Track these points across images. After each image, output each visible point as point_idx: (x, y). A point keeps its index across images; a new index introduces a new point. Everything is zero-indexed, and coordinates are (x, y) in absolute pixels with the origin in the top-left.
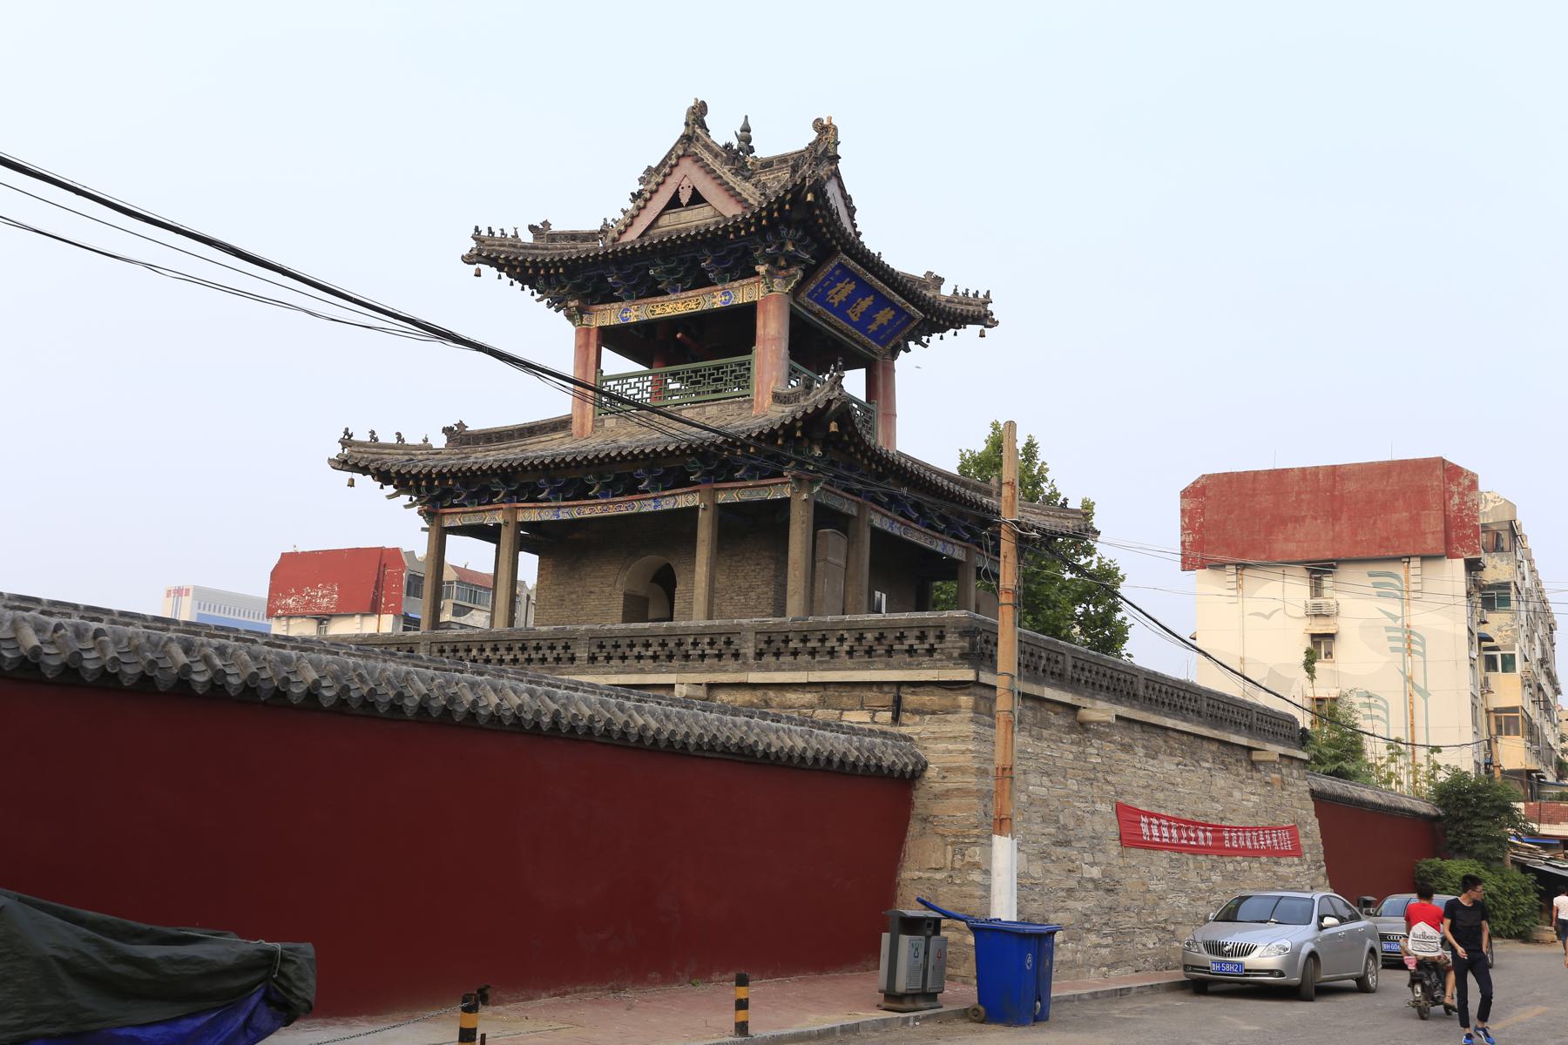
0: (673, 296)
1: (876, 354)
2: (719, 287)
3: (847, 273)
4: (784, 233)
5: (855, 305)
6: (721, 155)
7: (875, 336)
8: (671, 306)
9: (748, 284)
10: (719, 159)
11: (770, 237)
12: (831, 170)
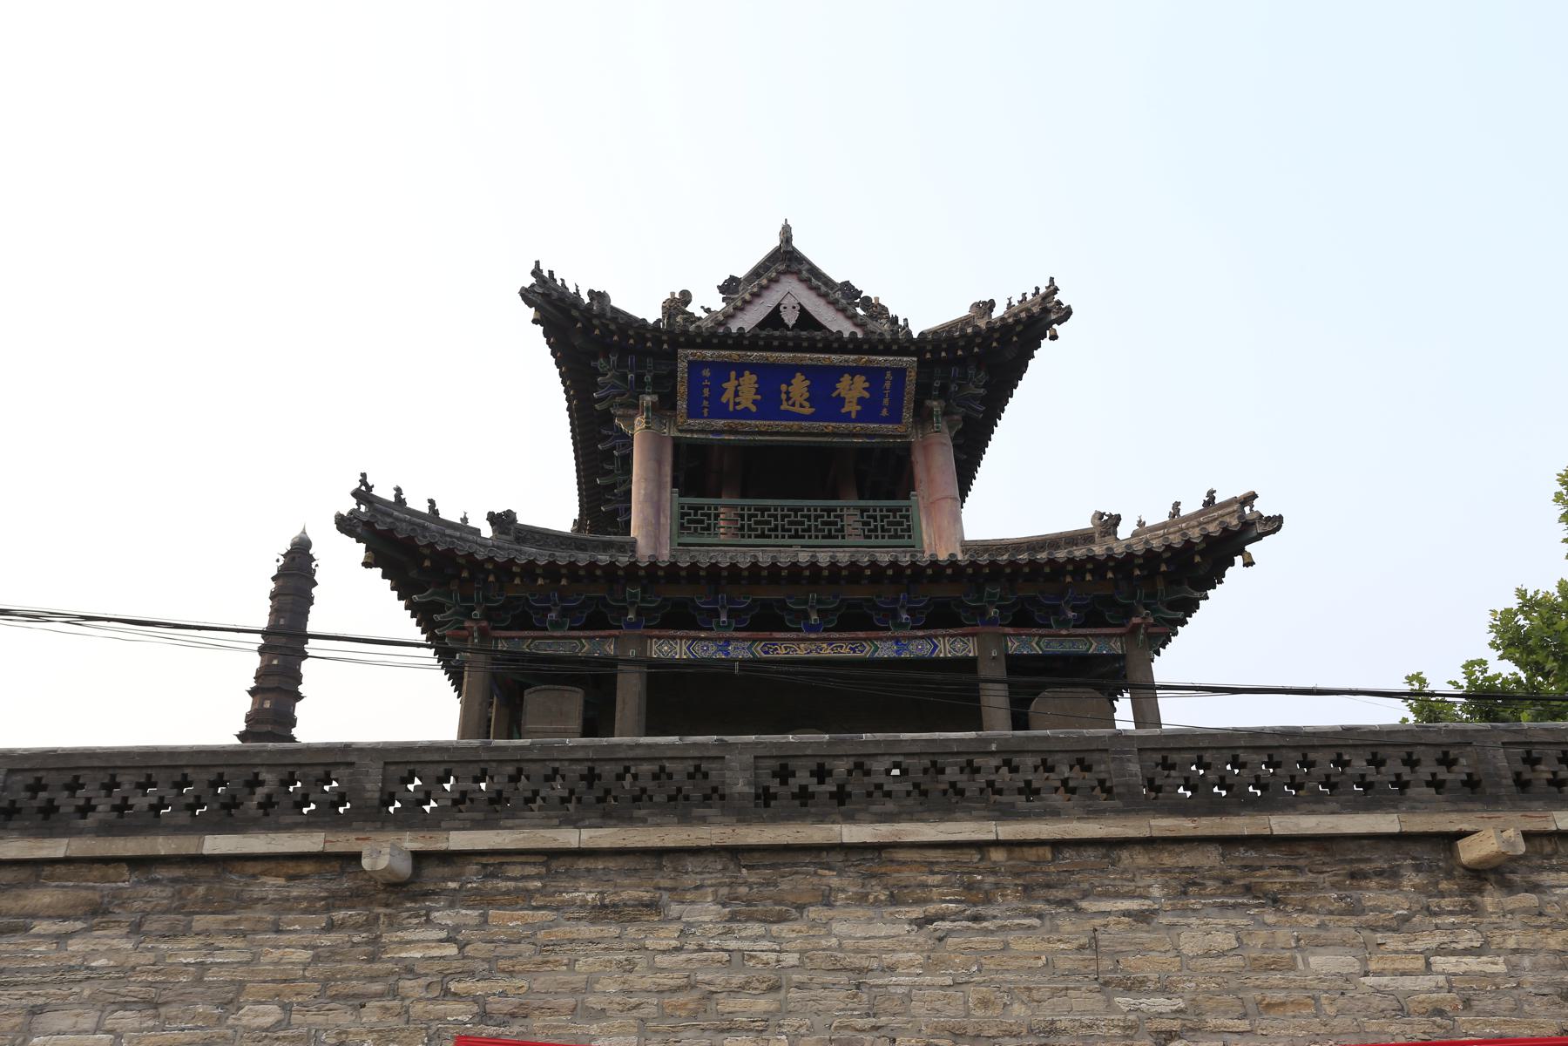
1: (906, 437)
3: (722, 371)
5: (784, 396)
7: (861, 417)
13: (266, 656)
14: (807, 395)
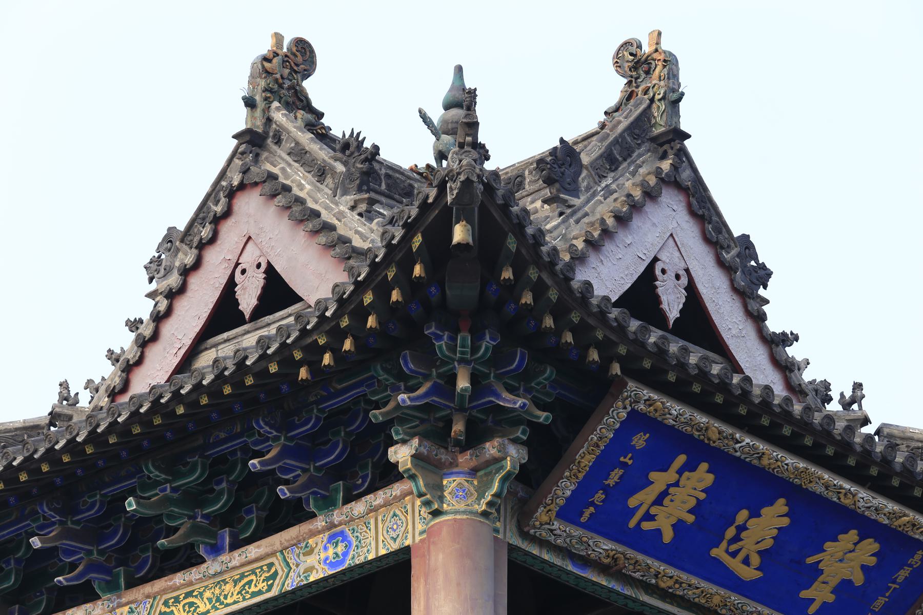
0: (212, 566)
2: (320, 522)
4: (442, 345)
5: (731, 532)
6: (333, 171)
8: (208, 594)
9: (387, 504)
10: (329, 180)
11: (409, 365)
12: (659, 171)
14: (768, 543)
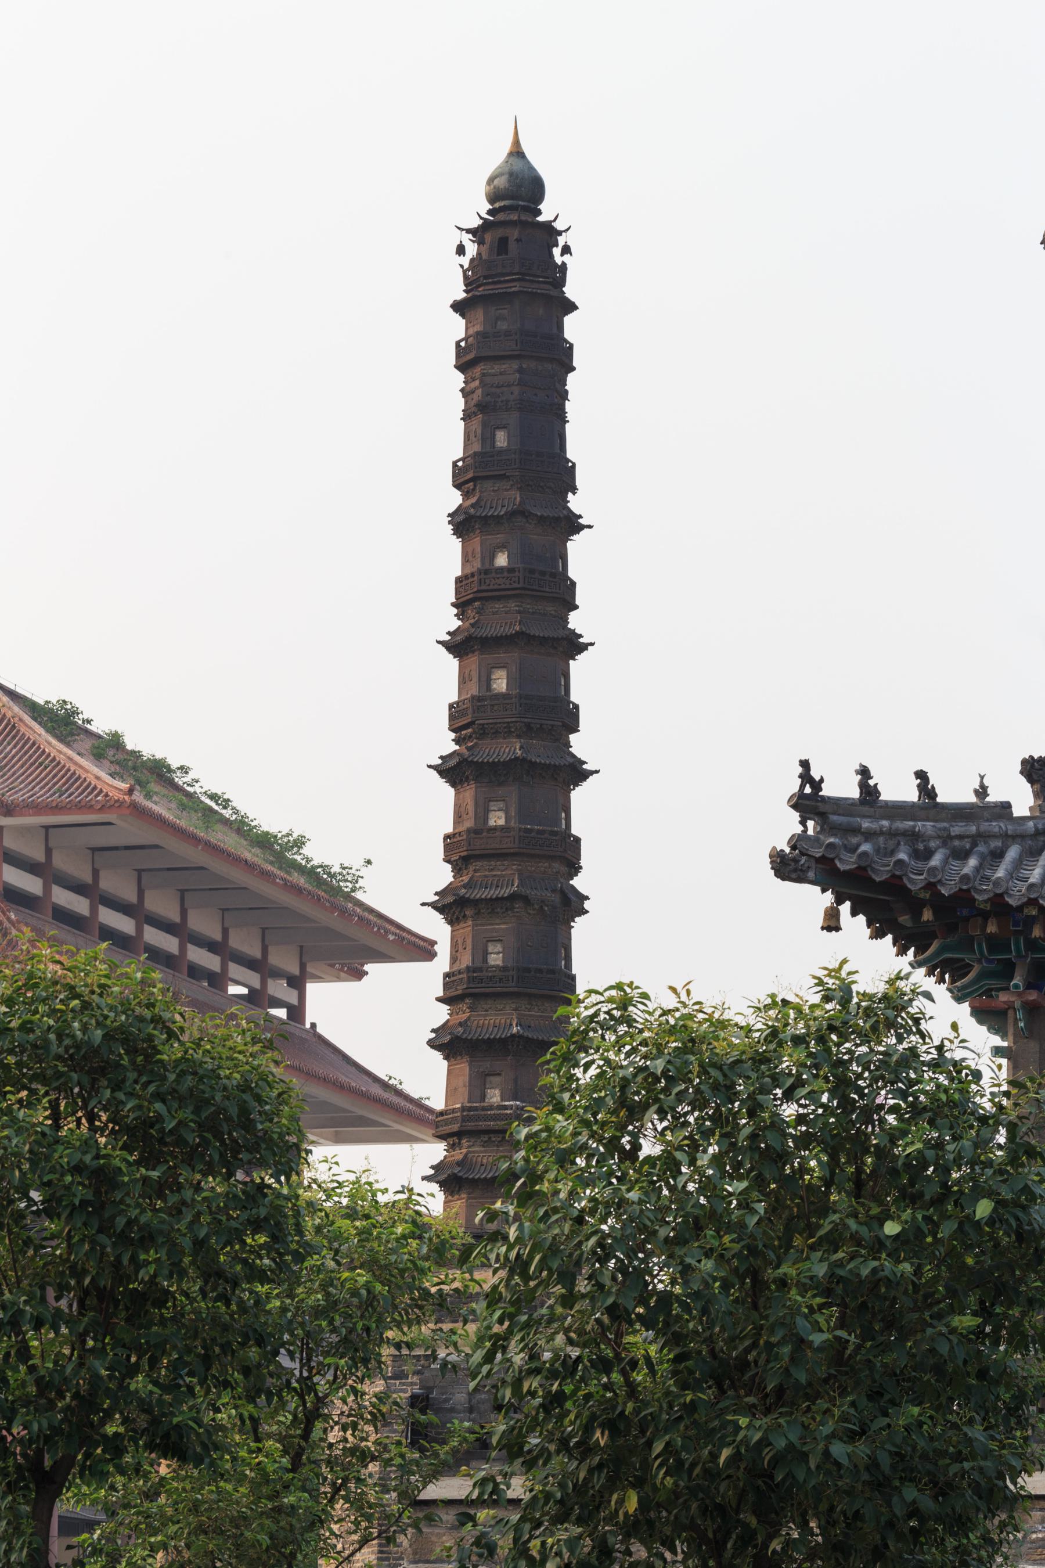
13: (476, 542)
